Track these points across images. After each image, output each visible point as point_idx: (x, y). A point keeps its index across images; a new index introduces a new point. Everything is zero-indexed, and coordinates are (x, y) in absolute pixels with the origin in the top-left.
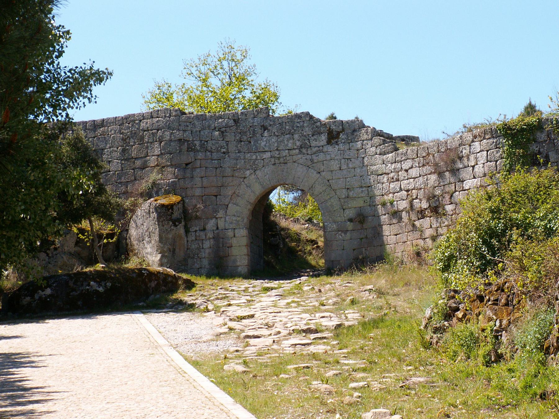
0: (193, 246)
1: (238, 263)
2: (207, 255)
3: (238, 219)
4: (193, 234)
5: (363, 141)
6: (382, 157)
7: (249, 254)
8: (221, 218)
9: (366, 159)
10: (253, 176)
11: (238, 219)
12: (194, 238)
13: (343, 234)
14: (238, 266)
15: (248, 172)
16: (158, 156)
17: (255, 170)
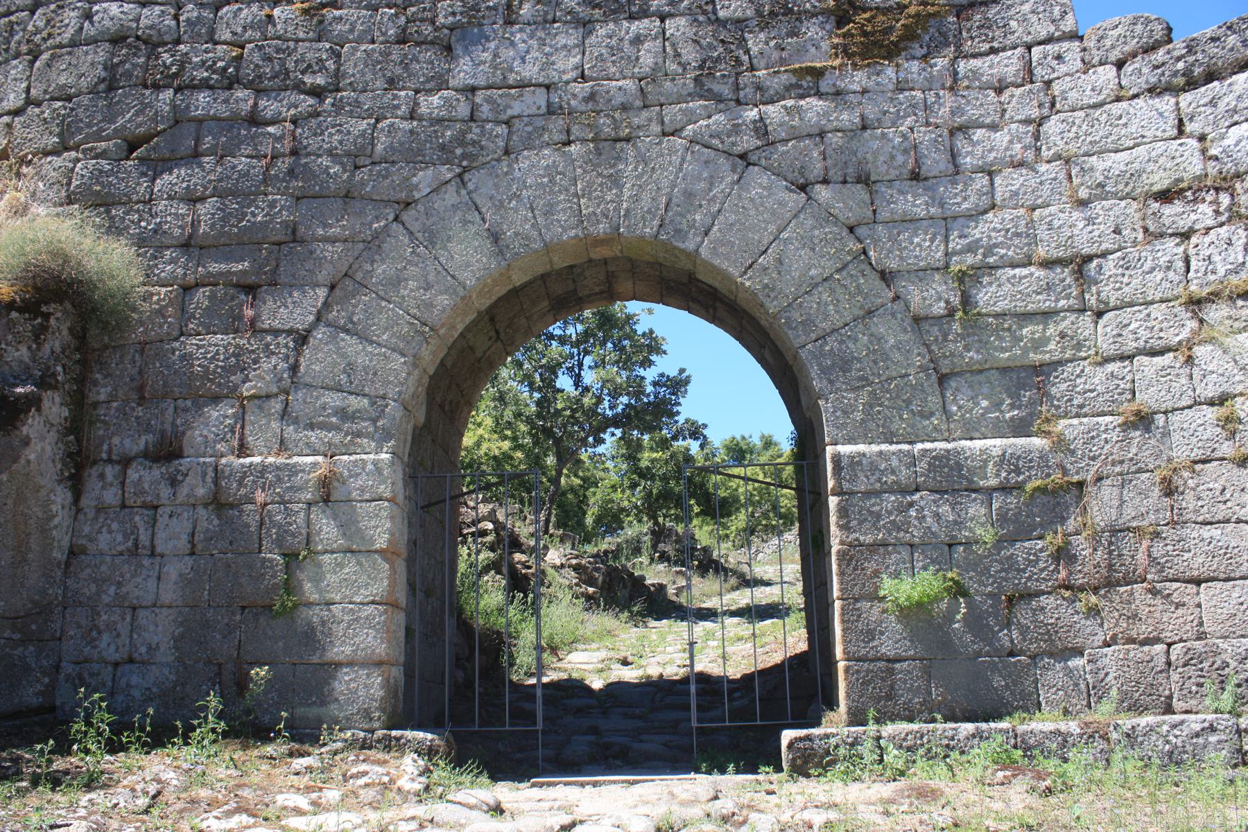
0: (104, 540)
1: (340, 650)
2: (169, 594)
3: (355, 403)
4: (110, 471)
5: (1029, 48)
6: (1166, 103)
7: (402, 598)
8: (268, 397)
9: (1052, 127)
10: (451, 196)
11: (355, 403)
12: (111, 496)
13: (945, 509)
14: (339, 665)
15: (424, 179)
16: (17, 112)
17: (466, 170)
